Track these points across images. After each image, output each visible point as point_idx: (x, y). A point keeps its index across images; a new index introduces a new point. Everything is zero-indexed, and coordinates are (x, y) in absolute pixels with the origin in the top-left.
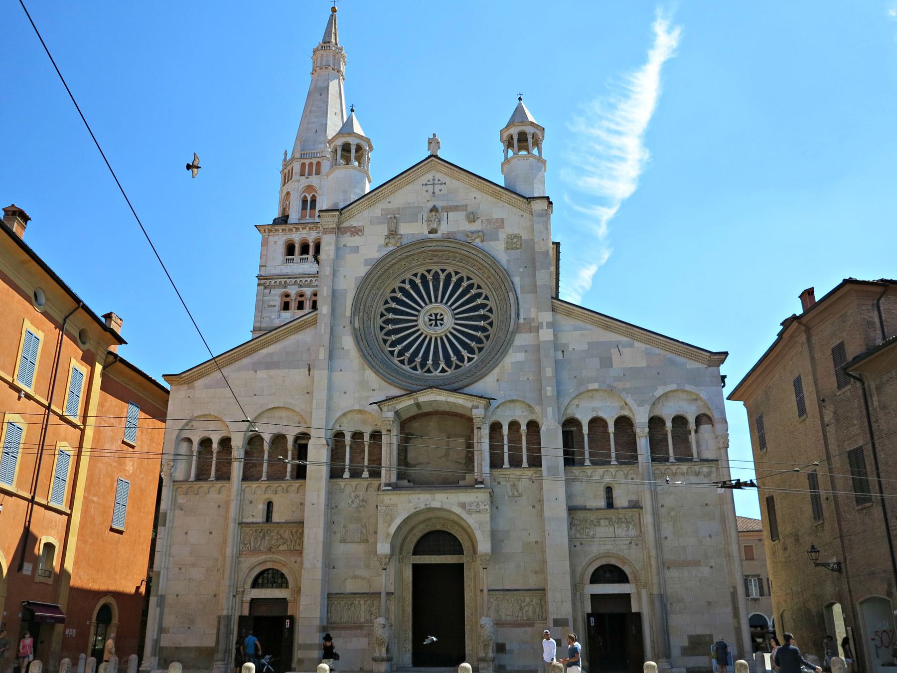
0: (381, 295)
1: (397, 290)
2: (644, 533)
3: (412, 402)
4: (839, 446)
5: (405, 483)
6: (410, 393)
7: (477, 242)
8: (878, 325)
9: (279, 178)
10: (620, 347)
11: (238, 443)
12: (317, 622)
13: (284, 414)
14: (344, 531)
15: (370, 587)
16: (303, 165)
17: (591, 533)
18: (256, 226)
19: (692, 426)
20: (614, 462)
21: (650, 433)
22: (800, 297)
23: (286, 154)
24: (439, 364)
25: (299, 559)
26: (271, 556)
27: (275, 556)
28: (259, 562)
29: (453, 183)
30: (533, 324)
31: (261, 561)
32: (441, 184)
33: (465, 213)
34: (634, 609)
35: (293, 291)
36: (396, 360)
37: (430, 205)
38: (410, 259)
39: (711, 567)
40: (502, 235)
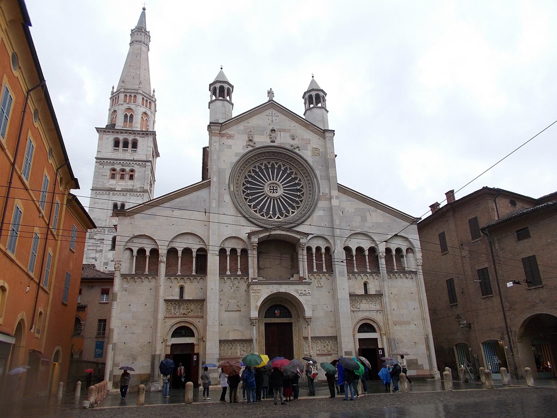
0: (243, 174)
1: (252, 172)
2: (384, 307)
3: (268, 234)
4: (471, 267)
5: (261, 278)
6: (266, 229)
7: (297, 151)
8: (495, 210)
9: (108, 102)
10: (370, 212)
11: (163, 252)
12: (217, 356)
13: (190, 237)
14: (227, 304)
15: (243, 335)
16: (126, 95)
18: (96, 128)
19: (404, 253)
20: (369, 271)
21: (385, 256)
22: (446, 194)
23: (113, 88)
24: (276, 214)
25: (201, 320)
27: (186, 319)
28: (176, 322)
29: (282, 117)
30: (327, 196)
31: (178, 321)
32: (276, 116)
33: (289, 134)
34: (380, 346)
35: (118, 168)
36: (252, 211)
37: (271, 128)
40: (310, 148)
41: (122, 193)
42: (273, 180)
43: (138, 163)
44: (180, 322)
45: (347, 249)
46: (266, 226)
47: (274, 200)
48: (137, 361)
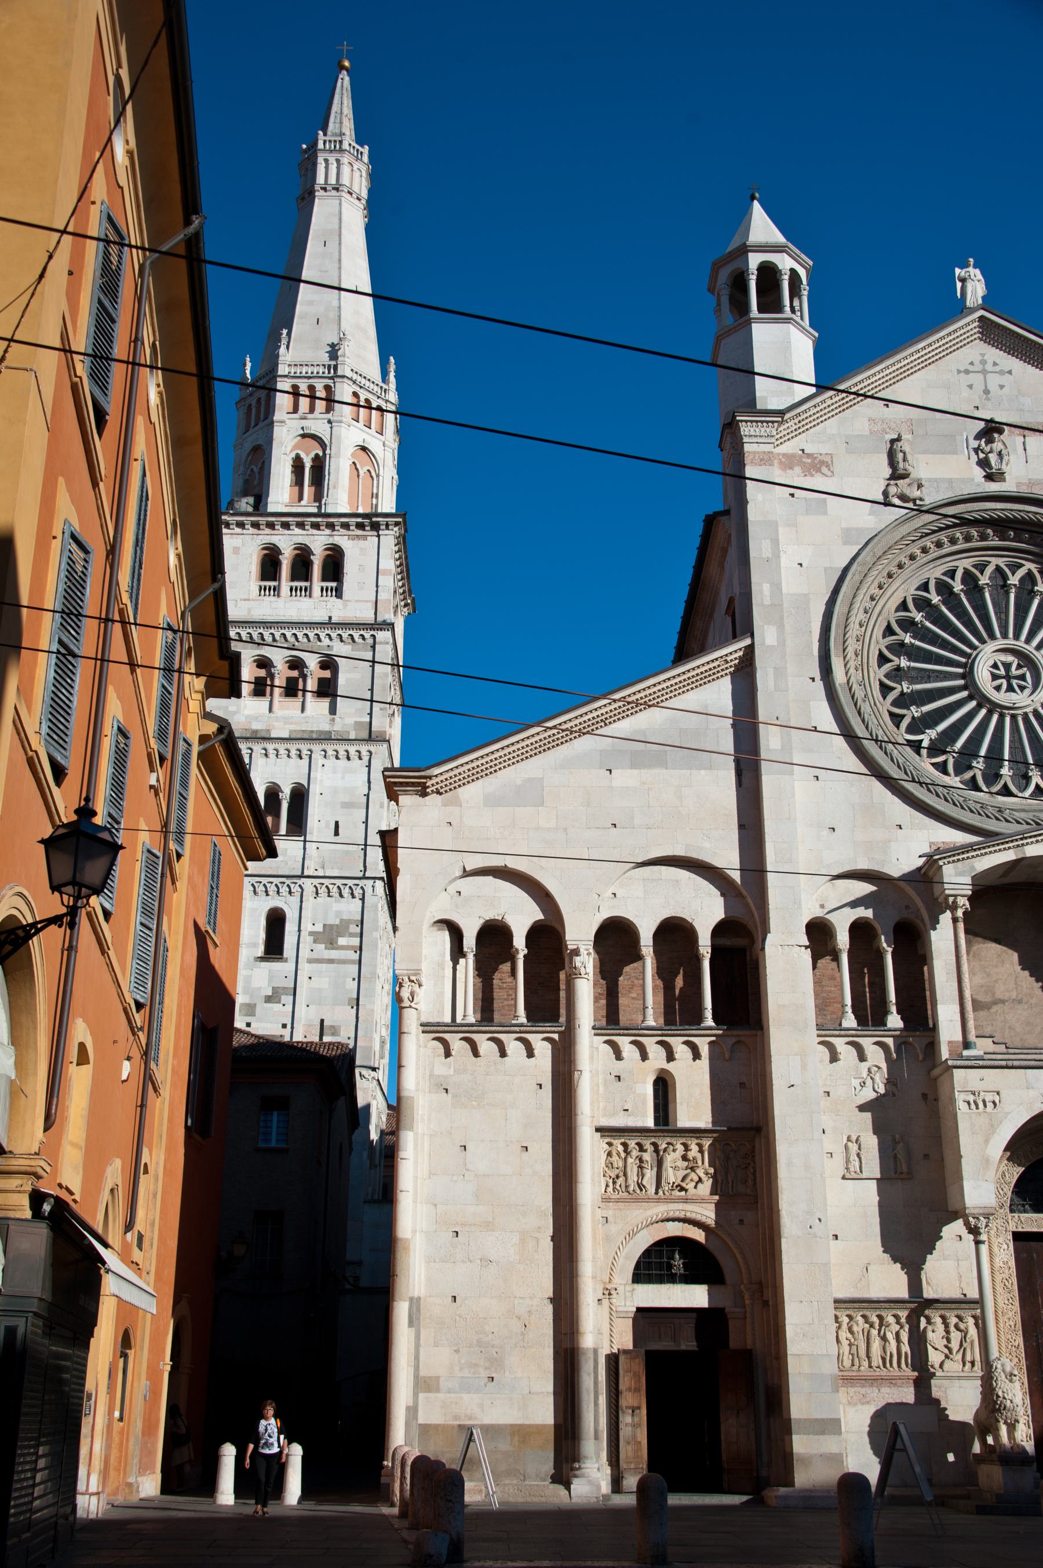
3: (1008, 856)
12: (830, 1368)
14: (853, 1147)
24: (1027, 779)
26: (681, 1206)
27: (689, 1207)
38: (943, 537)
41: (293, 747)
42: (1005, 636)
43: (345, 636)
46: (991, 825)
47: (1014, 717)
48: (507, 1373)
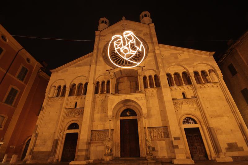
12: (86, 141)
17: (180, 107)
19: (208, 73)
20: (184, 84)
39: (228, 117)
40: (142, 33)
44: (73, 120)
45: (169, 75)
